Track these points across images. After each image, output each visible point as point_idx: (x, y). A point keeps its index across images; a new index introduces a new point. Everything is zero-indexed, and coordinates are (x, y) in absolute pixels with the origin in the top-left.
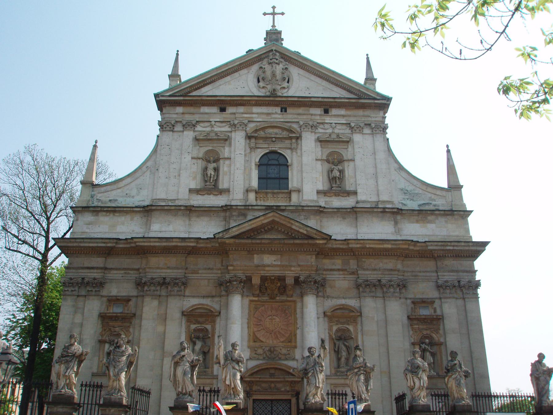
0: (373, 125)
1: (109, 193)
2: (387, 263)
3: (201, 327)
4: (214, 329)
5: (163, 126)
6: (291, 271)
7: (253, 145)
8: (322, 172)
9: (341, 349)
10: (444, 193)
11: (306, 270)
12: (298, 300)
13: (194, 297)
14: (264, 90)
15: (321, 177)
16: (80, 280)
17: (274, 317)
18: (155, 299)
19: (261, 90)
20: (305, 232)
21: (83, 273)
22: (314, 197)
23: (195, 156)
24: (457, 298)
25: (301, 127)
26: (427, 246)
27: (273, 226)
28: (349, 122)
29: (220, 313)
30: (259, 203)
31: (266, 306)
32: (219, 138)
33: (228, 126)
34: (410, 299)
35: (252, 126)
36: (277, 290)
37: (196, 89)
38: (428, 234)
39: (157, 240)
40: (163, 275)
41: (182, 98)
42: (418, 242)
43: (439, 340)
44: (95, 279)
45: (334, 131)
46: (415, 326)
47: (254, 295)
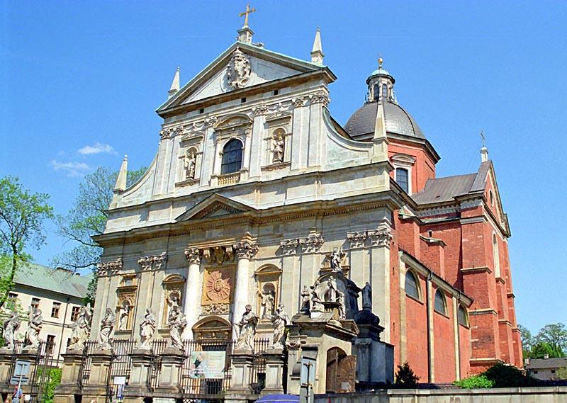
0: (311, 97)
10: (367, 149)
22: (259, 173)
26: (337, 203)
37: (185, 98)
41: (172, 110)
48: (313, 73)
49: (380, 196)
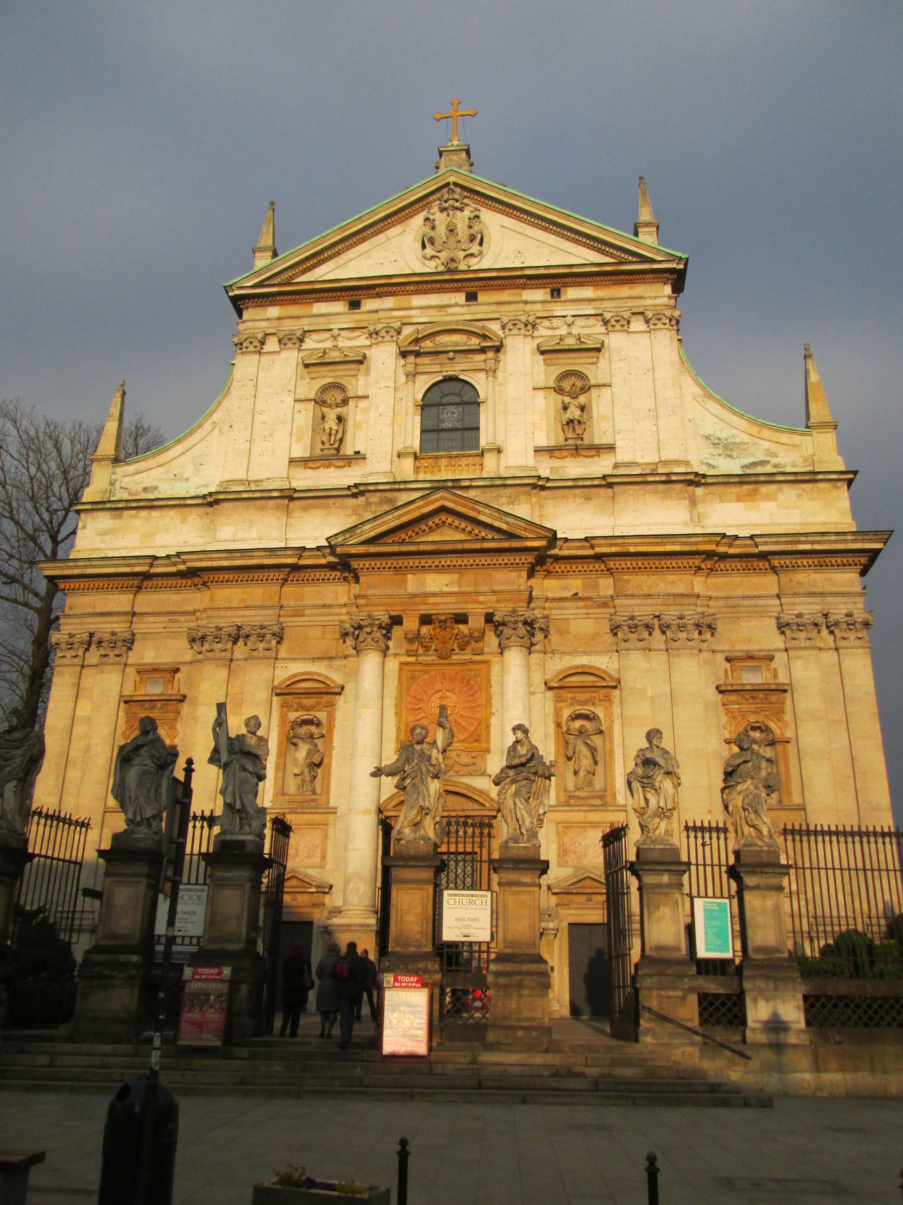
0: (649, 314)
1: (144, 474)
2: (673, 582)
3: (307, 717)
4: (331, 719)
5: (241, 344)
6: (479, 603)
7: (410, 368)
8: (547, 412)
9: (580, 753)
10: (796, 439)
11: (508, 601)
12: (495, 659)
13: (295, 659)
14: (433, 264)
15: (544, 422)
16: (85, 637)
17: (448, 694)
18: (223, 666)
19: (427, 262)
20: (504, 527)
21: (91, 623)
22: (530, 460)
23: (302, 397)
24: (820, 649)
25: (503, 327)
27: (443, 518)
28: (600, 312)
29: (343, 688)
30: (421, 477)
31: (433, 673)
32: (347, 359)
33: (364, 337)
34: (723, 652)
35: (407, 331)
36: (451, 642)
38: (759, 522)
39: (225, 555)
40: (238, 621)
42: (736, 537)
43: (782, 733)
44: (114, 634)
45: (570, 331)
46: (732, 706)
47: (409, 653)
48: (655, 266)
49: (863, 541)
